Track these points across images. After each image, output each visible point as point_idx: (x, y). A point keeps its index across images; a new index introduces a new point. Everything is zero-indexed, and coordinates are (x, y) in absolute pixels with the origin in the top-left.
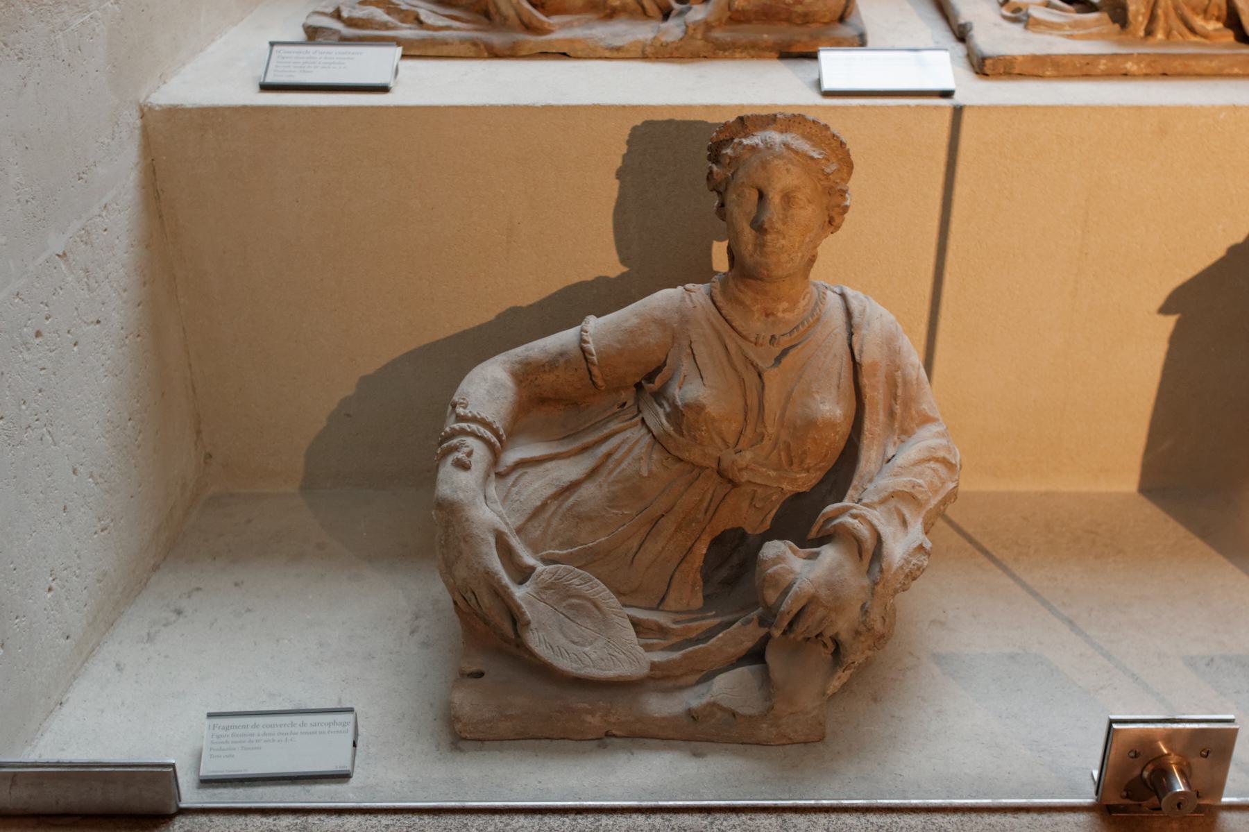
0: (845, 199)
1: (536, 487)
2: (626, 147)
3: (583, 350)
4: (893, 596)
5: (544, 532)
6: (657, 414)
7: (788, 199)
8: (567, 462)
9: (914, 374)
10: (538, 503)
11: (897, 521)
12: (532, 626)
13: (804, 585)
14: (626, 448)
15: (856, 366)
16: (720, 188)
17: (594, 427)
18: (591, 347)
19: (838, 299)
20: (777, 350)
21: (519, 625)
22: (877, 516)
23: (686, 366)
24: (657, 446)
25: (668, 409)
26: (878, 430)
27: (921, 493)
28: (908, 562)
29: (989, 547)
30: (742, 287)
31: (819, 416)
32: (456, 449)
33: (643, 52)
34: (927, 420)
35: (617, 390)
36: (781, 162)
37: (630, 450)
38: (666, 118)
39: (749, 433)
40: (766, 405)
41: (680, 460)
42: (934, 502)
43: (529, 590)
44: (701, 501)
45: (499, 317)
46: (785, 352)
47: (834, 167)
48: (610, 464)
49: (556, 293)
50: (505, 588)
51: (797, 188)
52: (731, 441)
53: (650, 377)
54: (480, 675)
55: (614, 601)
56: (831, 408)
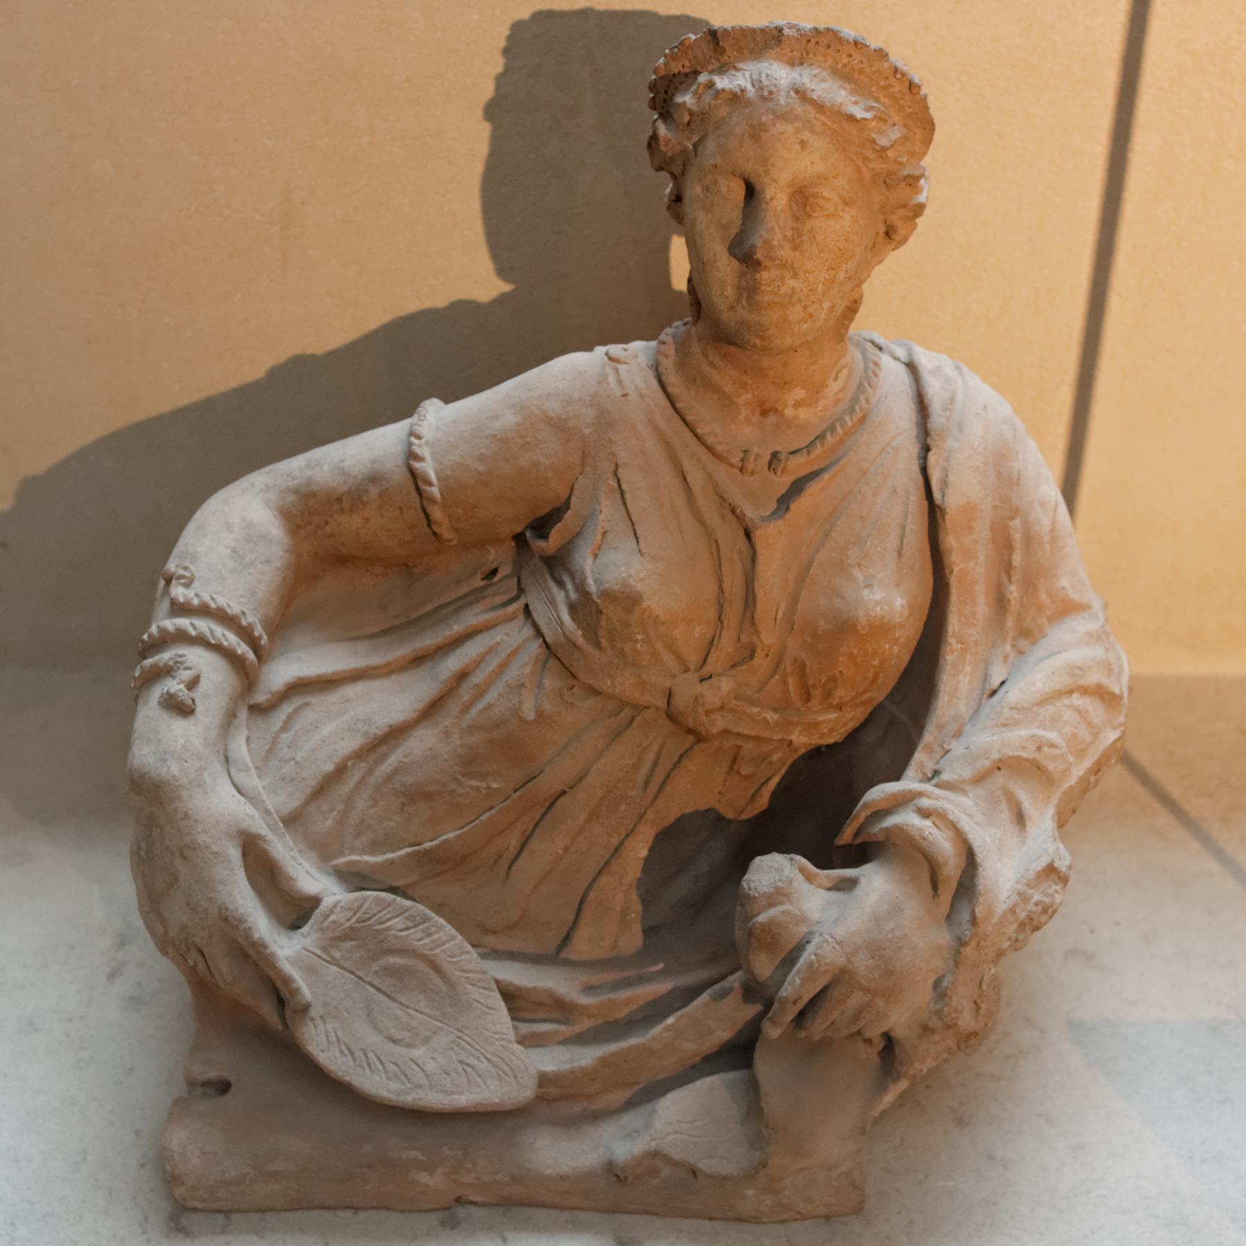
0: (918, 191)
1: (329, 732)
3: (413, 474)
4: (995, 962)
5: (340, 823)
6: (552, 602)
7: (804, 199)
8: (385, 683)
9: (1045, 524)
10: (329, 767)
11: (1005, 815)
12: (314, 1012)
13: (827, 950)
14: (494, 662)
15: (934, 512)
16: (675, 167)
17: (437, 616)
18: (428, 468)
19: (902, 371)
20: (783, 482)
21: (288, 1013)
22: (966, 810)
23: (607, 513)
24: (552, 662)
25: (573, 596)
26: (974, 634)
27: (1053, 758)
28: (1025, 898)
29: (1176, 792)
30: (717, 361)
31: (863, 621)
32: (166, 672)
34: (1067, 608)
35: (482, 544)
36: (788, 128)
37: (503, 666)
39: (727, 643)
40: (760, 593)
41: (596, 692)
42: (1078, 772)
43: (307, 942)
44: (636, 767)
45: (274, 373)
46: (797, 487)
47: (895, 134)
48: (465, 694)
49: (376, 332)
50: (260, 946)
51: (822, 178)
52: (694, 659)
53: (542, 526)
54: (223, 1087)
55: (470, 957)
56: (885, 596)
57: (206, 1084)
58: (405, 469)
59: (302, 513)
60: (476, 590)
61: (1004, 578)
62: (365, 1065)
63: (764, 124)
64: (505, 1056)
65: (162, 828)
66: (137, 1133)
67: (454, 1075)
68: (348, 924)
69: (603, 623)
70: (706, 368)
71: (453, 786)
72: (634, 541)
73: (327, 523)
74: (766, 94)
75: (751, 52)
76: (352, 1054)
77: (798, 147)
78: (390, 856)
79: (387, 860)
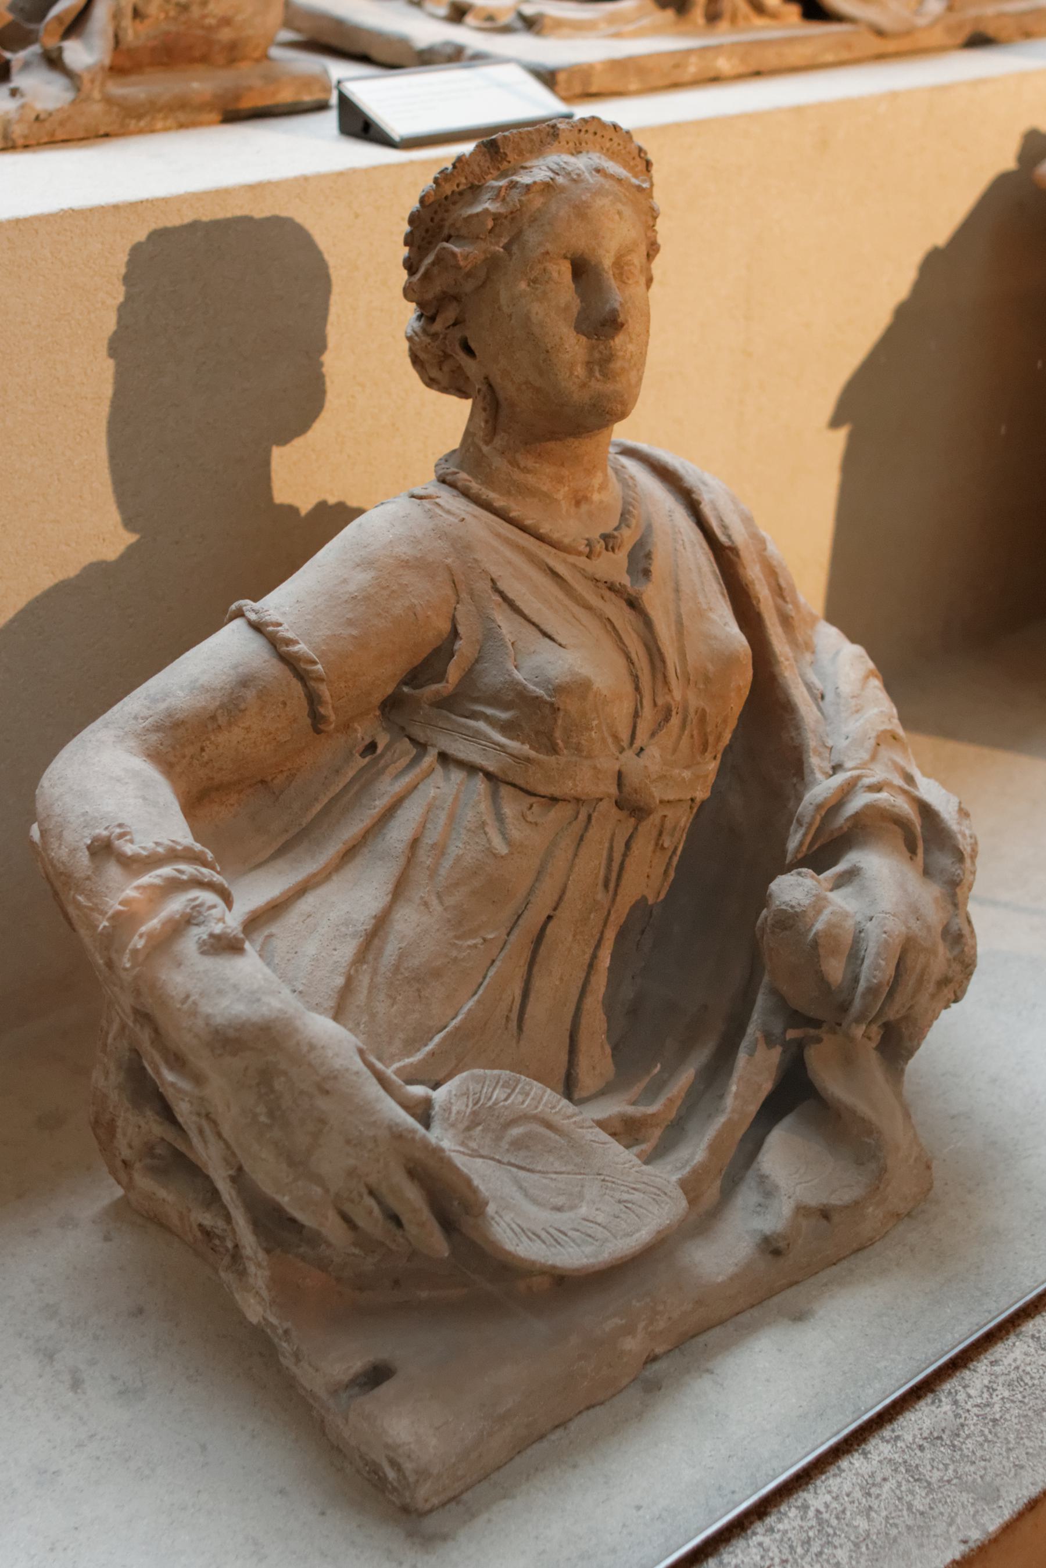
2: (122, 289)
8: (336, 881)
10: (340, 981)
14: (443, 817)
23: (506, 624)
24: (505, 791)
30: (530, 463)
38: (187, 220)
41: (554, 800)
48: (425, 858)
52: (625, 735)
58: (275, 661)
60: (363, 769)
62: (554, 1243)
63: (585, 202)
65: (285, 1073)
66: (282, 1492)
68: (469, 1110)
69: (560, 722)
71: (454, 953)
72: (547, 640)
74: (575, 177)
75: (531, 152)
76: (539, 1237)
77: (617, 217)
78: (431, 1046)
79: (428, 1054)
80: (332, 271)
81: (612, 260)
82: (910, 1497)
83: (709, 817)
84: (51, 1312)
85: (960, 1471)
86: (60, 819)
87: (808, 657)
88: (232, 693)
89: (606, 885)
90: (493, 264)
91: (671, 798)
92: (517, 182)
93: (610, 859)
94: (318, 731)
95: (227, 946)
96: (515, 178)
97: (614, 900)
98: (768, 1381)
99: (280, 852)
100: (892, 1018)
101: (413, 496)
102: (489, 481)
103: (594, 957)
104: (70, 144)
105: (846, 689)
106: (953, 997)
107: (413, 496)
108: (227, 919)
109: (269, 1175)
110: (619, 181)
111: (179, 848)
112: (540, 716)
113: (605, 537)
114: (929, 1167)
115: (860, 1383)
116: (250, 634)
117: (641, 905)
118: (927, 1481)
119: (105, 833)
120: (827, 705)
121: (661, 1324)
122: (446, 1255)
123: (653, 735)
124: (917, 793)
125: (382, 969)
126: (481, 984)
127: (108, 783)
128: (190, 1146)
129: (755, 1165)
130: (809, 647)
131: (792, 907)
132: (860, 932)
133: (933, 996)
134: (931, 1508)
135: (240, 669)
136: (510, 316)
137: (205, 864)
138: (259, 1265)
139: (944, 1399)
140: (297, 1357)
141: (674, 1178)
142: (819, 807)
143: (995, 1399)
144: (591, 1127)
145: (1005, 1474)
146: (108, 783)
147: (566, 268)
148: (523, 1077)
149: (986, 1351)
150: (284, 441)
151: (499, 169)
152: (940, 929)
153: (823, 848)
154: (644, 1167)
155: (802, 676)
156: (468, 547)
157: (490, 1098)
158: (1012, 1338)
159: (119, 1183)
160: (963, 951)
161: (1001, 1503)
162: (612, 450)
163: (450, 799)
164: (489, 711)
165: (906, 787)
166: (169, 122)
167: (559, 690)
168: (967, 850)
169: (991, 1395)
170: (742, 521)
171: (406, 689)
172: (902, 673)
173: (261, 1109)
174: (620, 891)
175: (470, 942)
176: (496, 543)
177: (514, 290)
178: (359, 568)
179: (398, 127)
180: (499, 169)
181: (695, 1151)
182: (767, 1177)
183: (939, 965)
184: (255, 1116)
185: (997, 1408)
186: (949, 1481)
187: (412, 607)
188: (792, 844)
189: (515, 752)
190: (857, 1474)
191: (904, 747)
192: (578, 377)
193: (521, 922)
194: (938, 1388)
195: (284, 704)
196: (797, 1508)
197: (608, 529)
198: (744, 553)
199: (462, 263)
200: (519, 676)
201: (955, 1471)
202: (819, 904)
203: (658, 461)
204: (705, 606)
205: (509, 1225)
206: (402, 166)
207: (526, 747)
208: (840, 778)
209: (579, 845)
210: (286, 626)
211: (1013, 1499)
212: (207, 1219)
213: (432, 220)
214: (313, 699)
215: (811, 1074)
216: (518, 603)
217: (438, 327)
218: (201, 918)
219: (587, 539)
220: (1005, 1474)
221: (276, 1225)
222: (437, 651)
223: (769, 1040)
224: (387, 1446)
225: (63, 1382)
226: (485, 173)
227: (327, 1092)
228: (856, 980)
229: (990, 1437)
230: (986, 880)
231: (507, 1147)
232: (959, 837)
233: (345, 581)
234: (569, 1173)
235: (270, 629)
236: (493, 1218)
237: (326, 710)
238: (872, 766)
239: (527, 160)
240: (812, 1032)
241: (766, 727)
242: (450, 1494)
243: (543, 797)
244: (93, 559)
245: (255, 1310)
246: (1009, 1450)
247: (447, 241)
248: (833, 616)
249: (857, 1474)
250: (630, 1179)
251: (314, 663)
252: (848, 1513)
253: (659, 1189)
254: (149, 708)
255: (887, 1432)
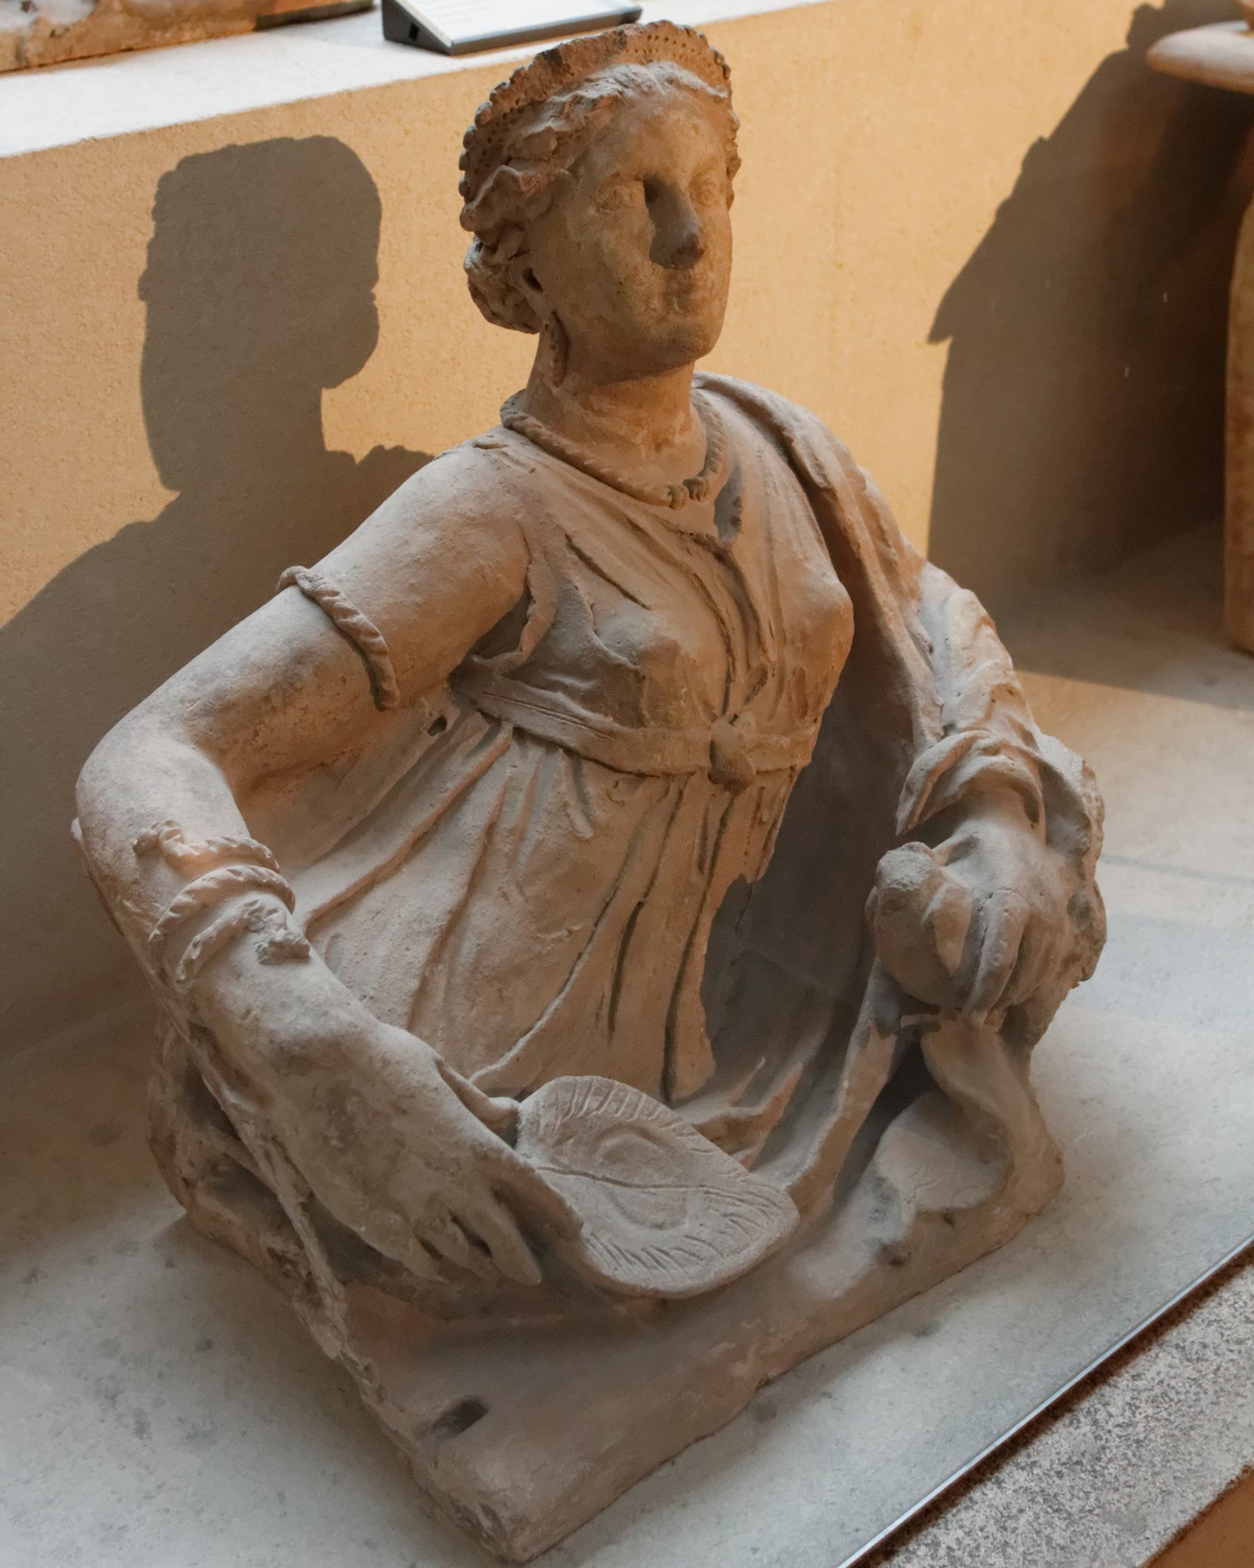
2: (152, 224)
6: (555, 707)
10: (414, 984)
14: (521, 798)
23: (584, 586)
24: (587, 768)
30: (605, 405)
33: (19, 55)
38: (220, 145)
39: (741, 676)
41: (641, 776)
48: (503, 845)
52: (717, 702)
57: (442, 1421)
58: (332, 634)
59: (225, 734)
61: (882, 545)
63: (658, 117)
64: (752, 1189)
65: (357, 1093)
67: (730, 1231)
68: (559, 1123)
69: (646, 690)
70: (592, 420)
71: (537, 948)
72: (629, 601)
73: (256, 734)
75: (596, 62)
76: (639, 1259)
77: (693, 133)
79: (512, 1059)
80: (381, 194)
81: (689, 179)
82: (1049, 1531)
83: (808, 784)
84: (110, 1348)
85: (1102, 1499)
86: (103, 817)
87: (914, 605)
88: (286, 671)
89: (700, 867)
90: (558, 189)
91: (770, 767)
92: (582, 97)
93: (704, 838)
94: (381, 709)
95: (289, 954)
96: (580, 93)
97: (709, 883)
98: (891, 1404)
99: (346, 842)
100: (1015, 1003)
101: (478, 446)
102: (559, 426)
103: (690, 944)
104: (90, 61)
105: (956, 640)
106: (1081, 975)
107: (478, 446)
108: (289, 924)
109: (341, 1201)
110: (694, 91)
111: (234, 846)
112: (624, 685)
113: (690, 484)
114: (1059, 1161)
115: (991, 1404)
116: (304, 604)
117: (739, 884)
118: (1066, 1511)
119: (153, 832)
120: (936, 658)
121: (773, 1347)
122: (539, 1281)
123: (748, 700)
124: (1037, 754)
125: (459, 970)
126: (568, 980)
127: (157, 780)
128: (256, 1165)
129: (870, 1168)
130: (915, 594)
131: (904, 885)
132: (979, 910)
133: (1060, 975)
134: (1073, 1542)
135: (294, 645)
136: (579, 245)
137: (263, 862)
138: (335, 1298)
139: (1082, 1419)
140: (380, 1393)
141: (783, 1186)
142: (930, 773)
143: (1139, 1417)
144: (692, 1134)
145: (1151, 1500)
146: (157, 780)
147: (638, 191)
148: (617, 1083)
149: (1127, 1364)
150: (334, 382)
151: (561, 82)
152: (1065, 903)
153: (938, 816)
154: (752, 1176)
155: (908, 626)
156: (539, 501)
157: (581, 1108)
158: (1155, 1349)
159: (181, 1203)
160: (1091, 926)
161: (1148, 1534)
162: (694, 384)
163: (528, 780)
164: (568, 681)
165: (1025, 748)
166: (198, 32)
167: (645, 656)
168: (1092, 814)
169: (1134, 1413)
170: (838, 457)
171: (476, 659)
172: (1016, 612)
173: (333, 1132)
174: (716, 870)
175: (555, 935)
176: (569, 495)
177: (585, 212)
178: (421, 528)
179: (449, 33)
180: (561, 82)
181: (805, 1155)
182: (884, 1180)
183: (1067, 940)
184: (326, 1139)
185: (1140, 1427)
186: (1091, 1511)
187: (480, 570)
188: (902, 814)
189: (598, 726)
190: (990, 1506)
191: (1022, 703)
192: (654, 310)
193: (609, 911)
194: (1076, 1407)
195: (344, 680)
196: (927, 1545)
197: (692, 474)
198: (841, 494)
199: (524, 188)
200: (599, 642)
201: (1097, 1499)
202: (934, 881)
203: (745, 394)
204: (800, 556)
205: (606, 1247)
206: (453, 75)
207: (610, 719)
208: (953, 740)
209: (669, 824)
210: (343, 595)
211: (1160, 1528)
212: (278, 1244)
213: (490, 140)
214: (375, 675)
215: (928, 1064)
216: (596, 561)
217: (498, 258)
218: (261, 924)
219: (670, 487)
220: (1151, 1500)
221: (352, 1256)
222: (509, 615)
223: (883, 1029)
224: (481, 1493)
225: (127, 1426)
226: (545, 88)
227: (404, 1112)
228: (976, 963)
229: (1134, 1460)
230: (1115, 834)
231: (601, 1160)
232: (1084, 800)
233: (406, 543)
234: (669, 1186)
235: (326, 598)
236: (588, 1241)
237: (391, 686)
238: (988, 726)
239: (593, 71)
240: (928, 1017)
241: (870, 686)
242: (549, 1542)
243: (630, 773)
244: (130, 520)
245: (332, 1345)
246: (1155, 1474)
247: (507, 164)
248: (940, 554)
249: (990, 1506)
250: (735, 1189)
251: (376, 635)
252: (982, 1550)
253: (767, 1199)
254: (196, 690)
255: (1021, 1459)
